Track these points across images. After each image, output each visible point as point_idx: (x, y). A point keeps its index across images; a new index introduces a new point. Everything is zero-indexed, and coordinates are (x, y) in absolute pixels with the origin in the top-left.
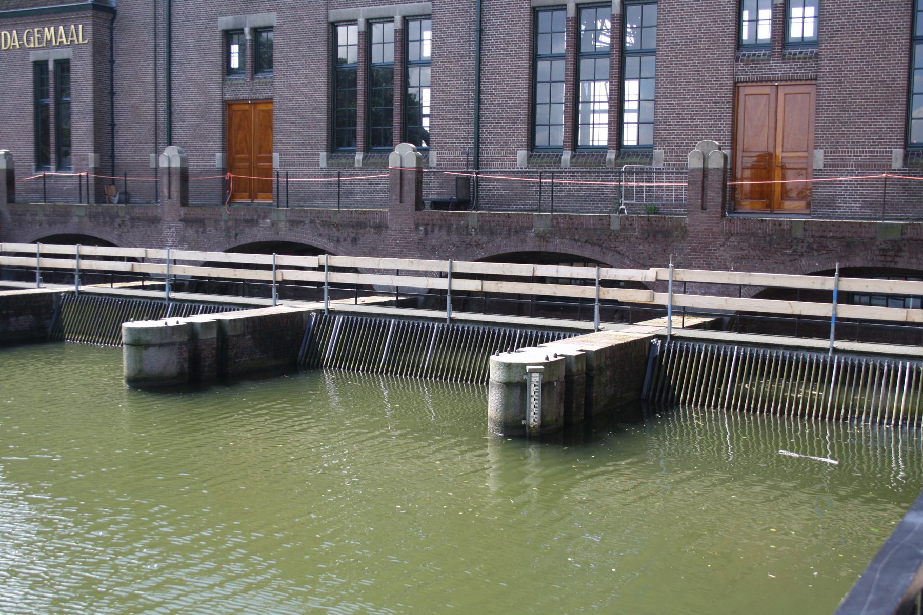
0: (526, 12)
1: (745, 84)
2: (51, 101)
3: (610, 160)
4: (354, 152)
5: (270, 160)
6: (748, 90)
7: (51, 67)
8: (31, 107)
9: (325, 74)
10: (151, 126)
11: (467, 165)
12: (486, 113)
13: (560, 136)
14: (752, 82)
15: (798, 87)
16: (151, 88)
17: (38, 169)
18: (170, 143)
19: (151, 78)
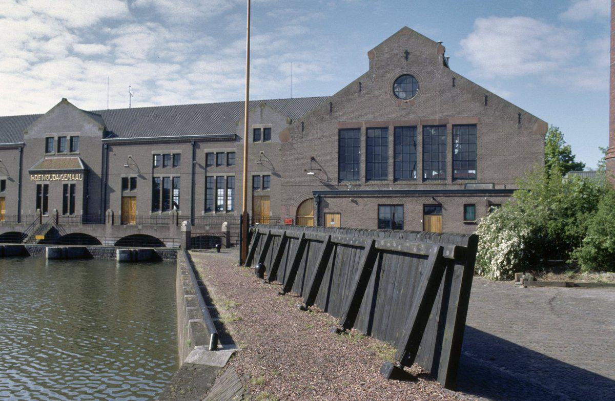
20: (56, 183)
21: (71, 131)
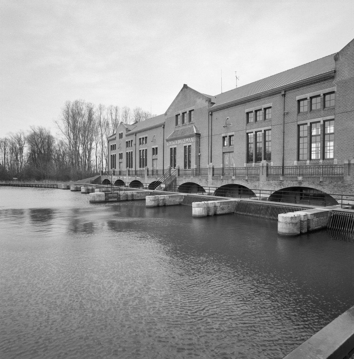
0: (296, 126)
4: (252, 163)
13: (306, 157)
18: (211, 162)
20: (180, 145)
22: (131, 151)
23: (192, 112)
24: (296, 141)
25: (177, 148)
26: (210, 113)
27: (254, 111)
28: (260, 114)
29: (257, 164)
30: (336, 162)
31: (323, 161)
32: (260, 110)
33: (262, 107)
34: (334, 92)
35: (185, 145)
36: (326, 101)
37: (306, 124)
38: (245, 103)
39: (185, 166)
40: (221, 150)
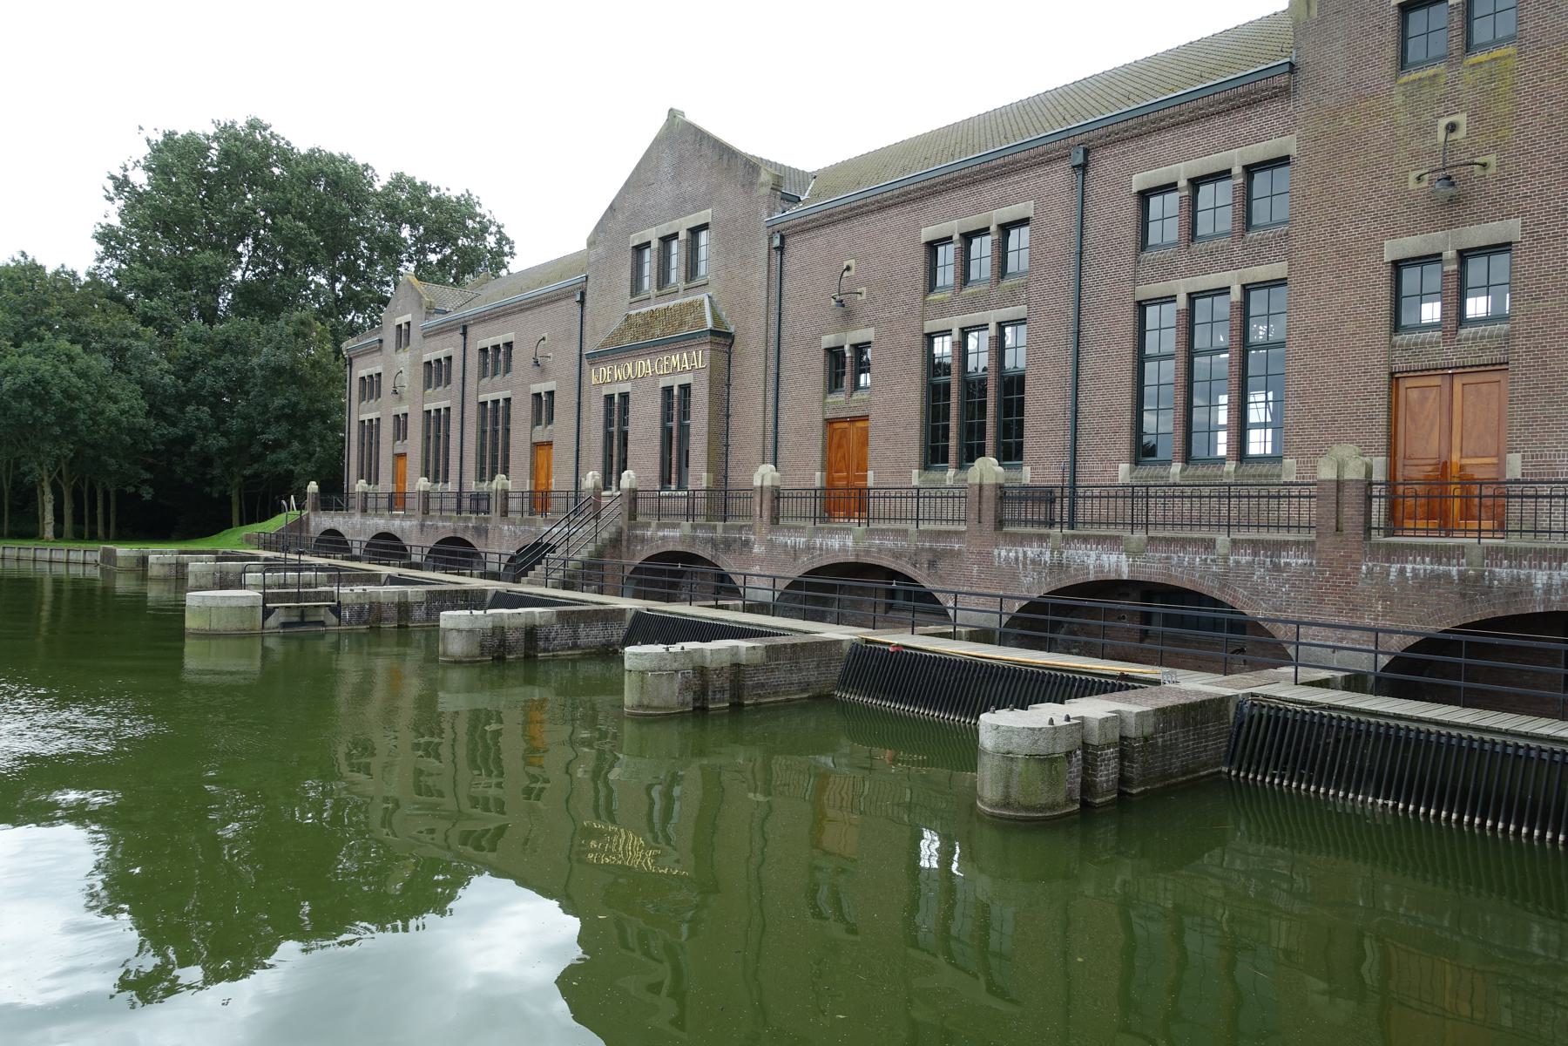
1: (1405, 374)
2: (674, 424)
3: (1228, 473)
4: (946, 469)
5: (865, 478)
6: (1409, 383)
7: (676, 392)
8: (658, 430)
9: (919, 389)
10: (759, 447)
11: (1063, 481)
12: (1084, 424)
14: (1415, 371)
15: (1482, 375)
16: (761, 408)
17: (663, 488)
19: (761, 400)
21: (689, 214)
22: (442, 405)
23: (704, 237)
24: (1127, 376)
25: (631, 396)
26: (777, 242)
27: (956, 237)
28: (982, 248)
29: (962, 475)
30: (1290, 469)
31: (1185, 470)
32: (983, 232)
33: (991, 216)
34: (1288, 157)
35: (664, 382)
36: (1254, 197)
37: (1172, 299)
38: (921, 198)
39: (665, 481)
40: (817, 406)
